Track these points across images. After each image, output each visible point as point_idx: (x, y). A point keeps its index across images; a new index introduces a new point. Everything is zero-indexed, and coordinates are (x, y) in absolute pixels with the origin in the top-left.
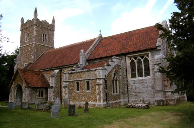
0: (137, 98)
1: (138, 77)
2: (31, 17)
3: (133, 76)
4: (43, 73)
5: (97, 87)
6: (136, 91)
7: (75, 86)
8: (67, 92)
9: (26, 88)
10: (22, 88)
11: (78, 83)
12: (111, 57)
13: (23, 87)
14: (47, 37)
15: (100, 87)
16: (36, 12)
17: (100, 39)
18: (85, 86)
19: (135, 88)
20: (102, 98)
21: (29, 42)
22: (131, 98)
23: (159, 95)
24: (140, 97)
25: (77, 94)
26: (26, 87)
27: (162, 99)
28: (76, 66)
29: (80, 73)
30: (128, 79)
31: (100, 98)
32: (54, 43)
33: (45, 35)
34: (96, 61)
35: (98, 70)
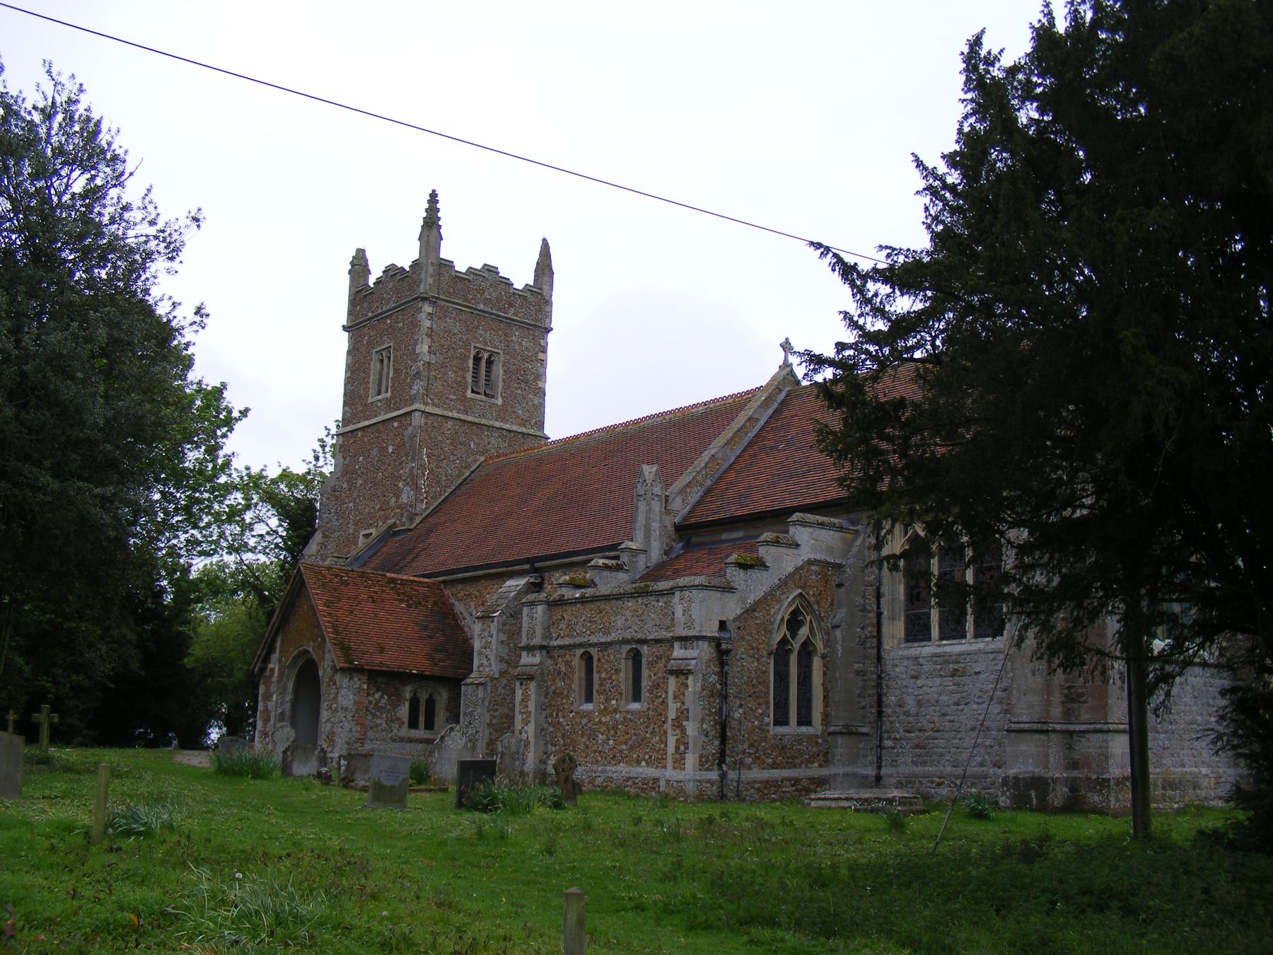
0: (924, 763)
1: (942, 637)
2: (406, 254)
3: (917, 631)
4: (448, 592)
5: (672, 683)
6: (924, 723)
7: (576, 677)
8: (532, 706)
9: (338, 677)
10: (320, 673)
11: (588, 658)
12: (778, 517)
13: (324, 671)
14: (499, 370)
15: (686, 686)
16: (431, 224)
17: (782, 396)
18: (622, 674)
19: (919, 703)
20: (691, 745)
21: (388, 404)
22: (894, 764)
23: (1023, 747)
24: (942, 755)
25: (584, 721)
26: (335, 670)
27: (1039, 771)
28: (601, 562)
29: (602, 605)
30: (886, 646)
31: (682, 748)
32: (542, 405)
33: (486, 356)
34: (725, 536)
35: (682, 588)
